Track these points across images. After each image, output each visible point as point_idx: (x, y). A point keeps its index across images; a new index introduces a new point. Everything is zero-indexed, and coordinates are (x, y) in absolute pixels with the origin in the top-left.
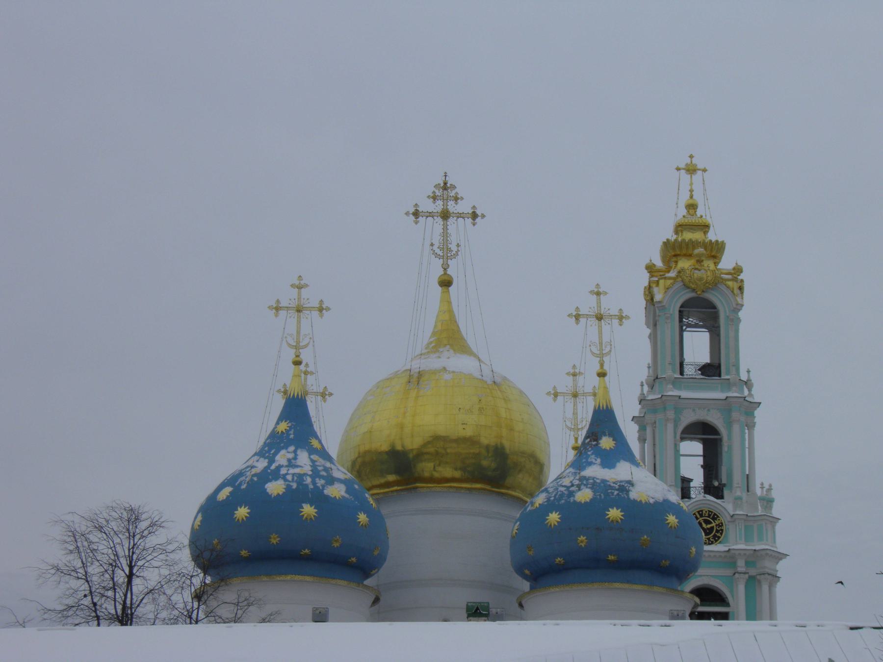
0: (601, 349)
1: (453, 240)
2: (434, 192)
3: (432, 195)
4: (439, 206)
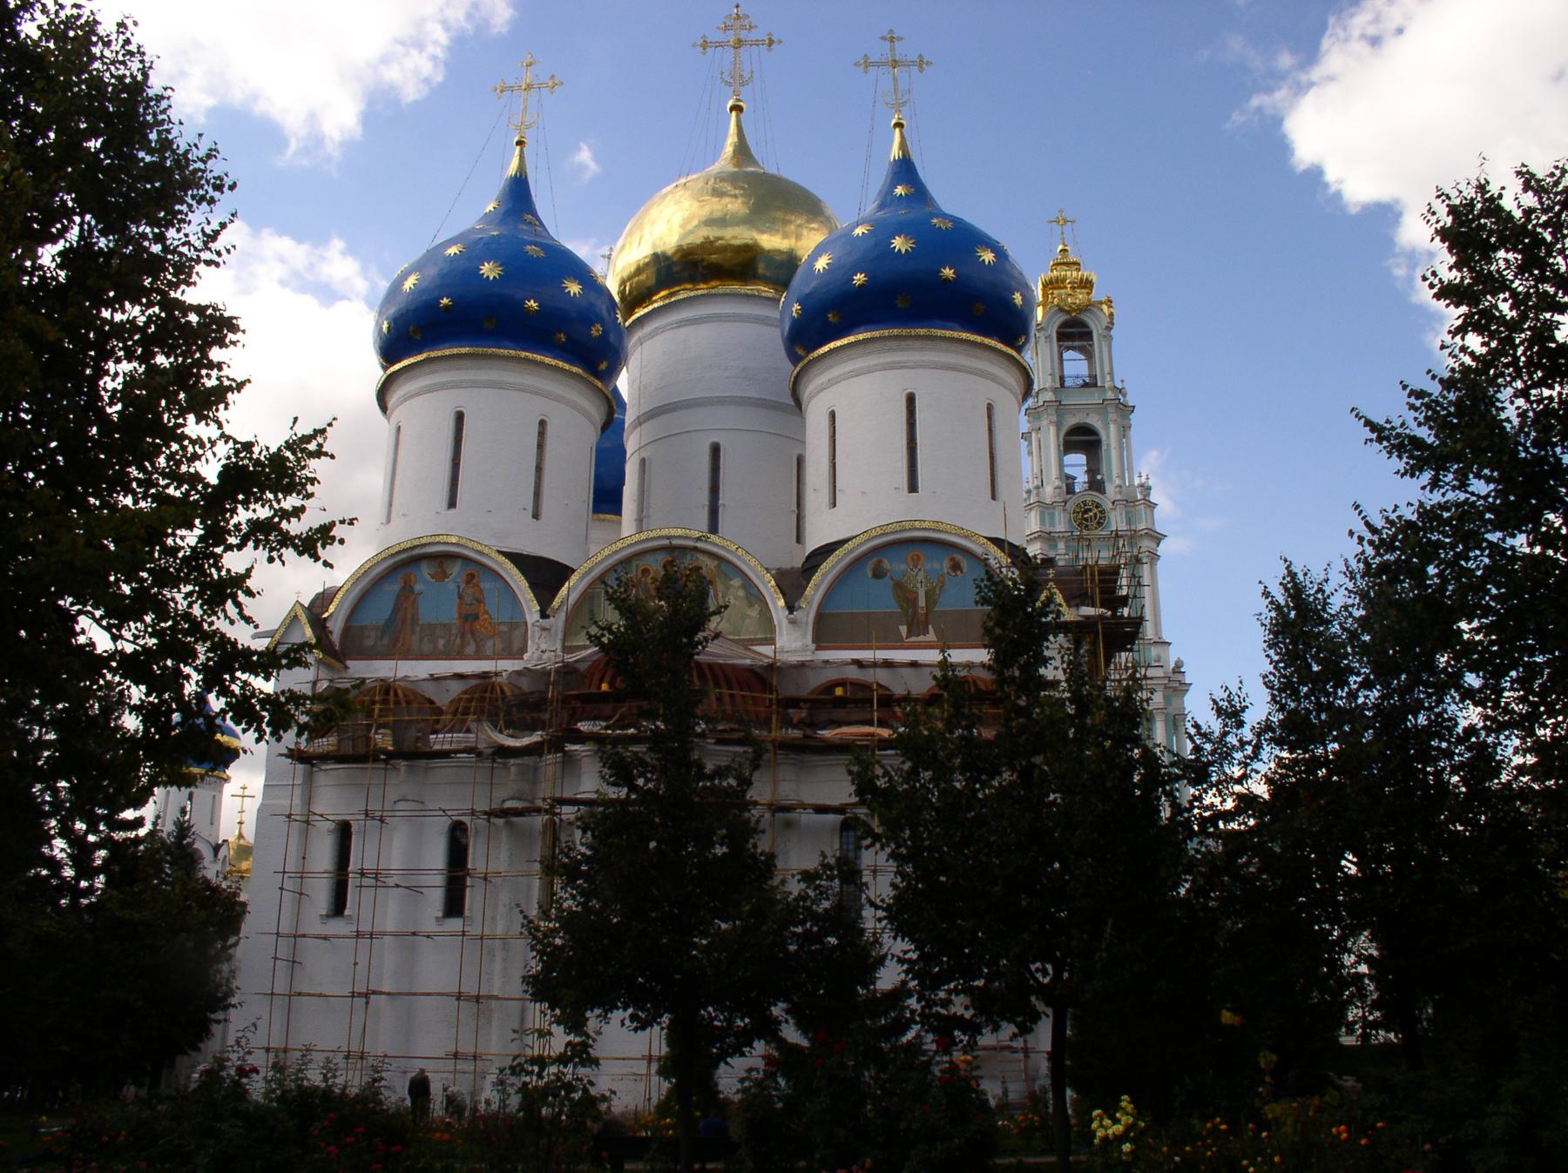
4: (731, 37)
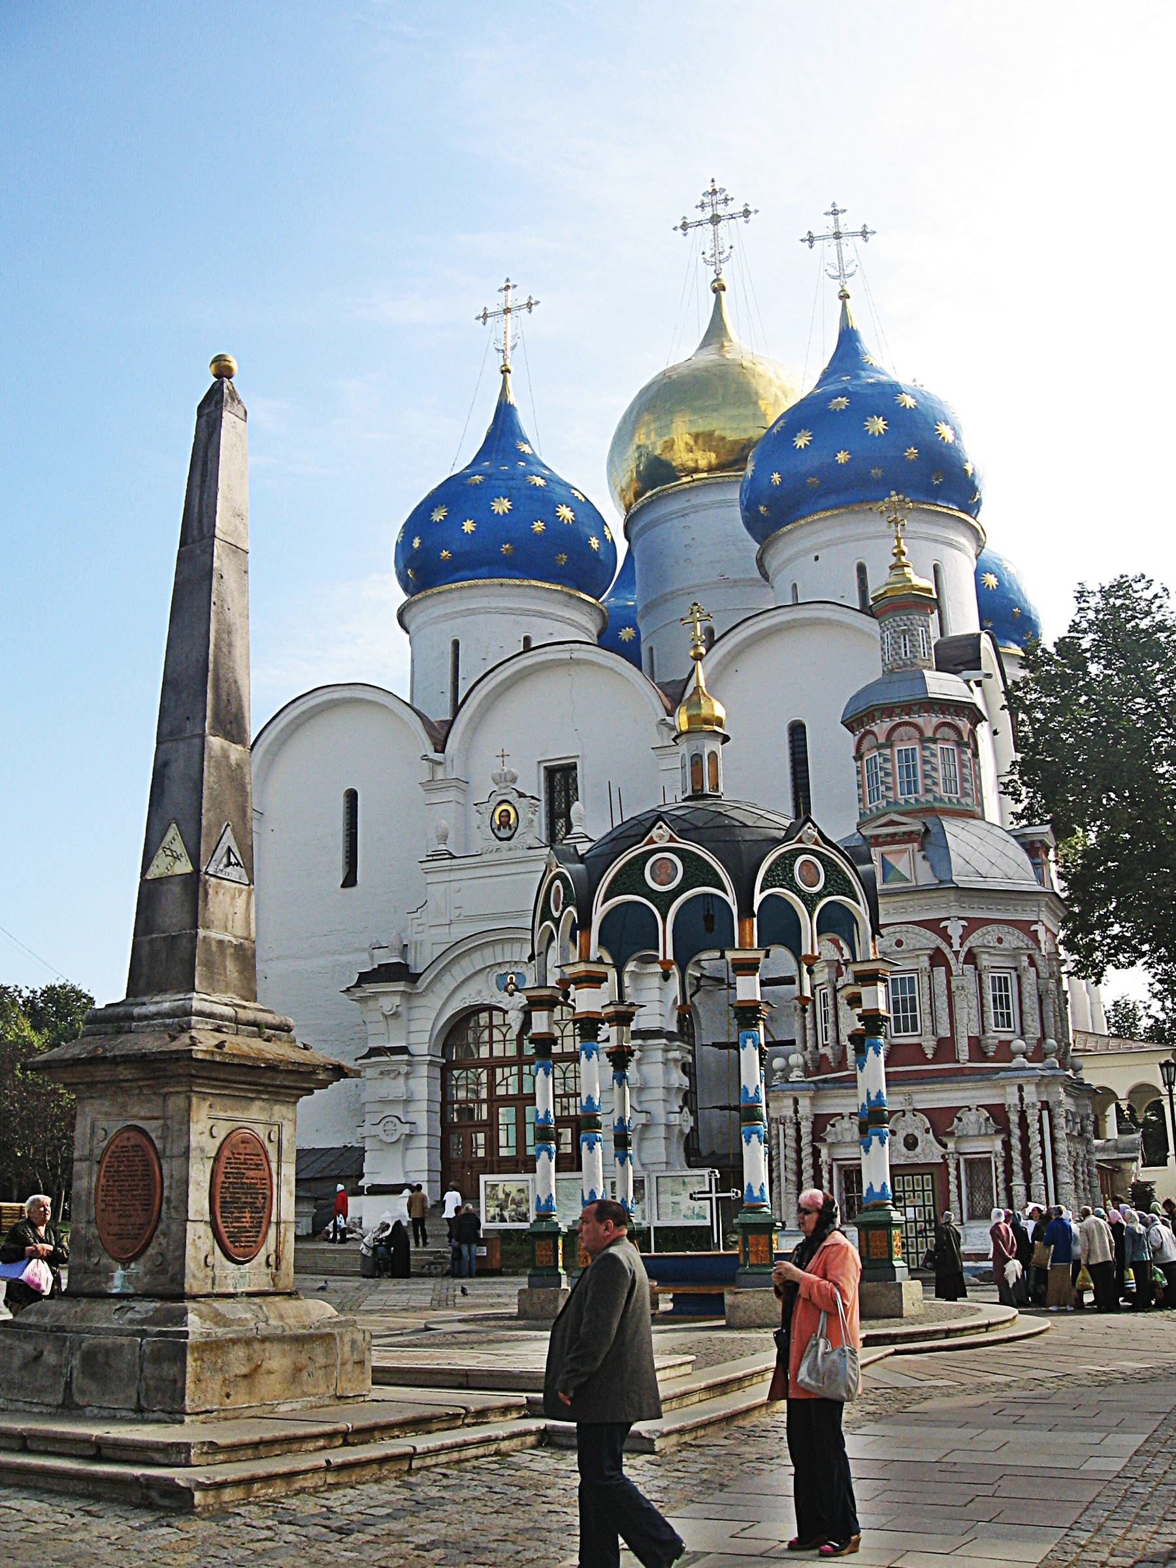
0: (841, 269)
1: (725, 244)
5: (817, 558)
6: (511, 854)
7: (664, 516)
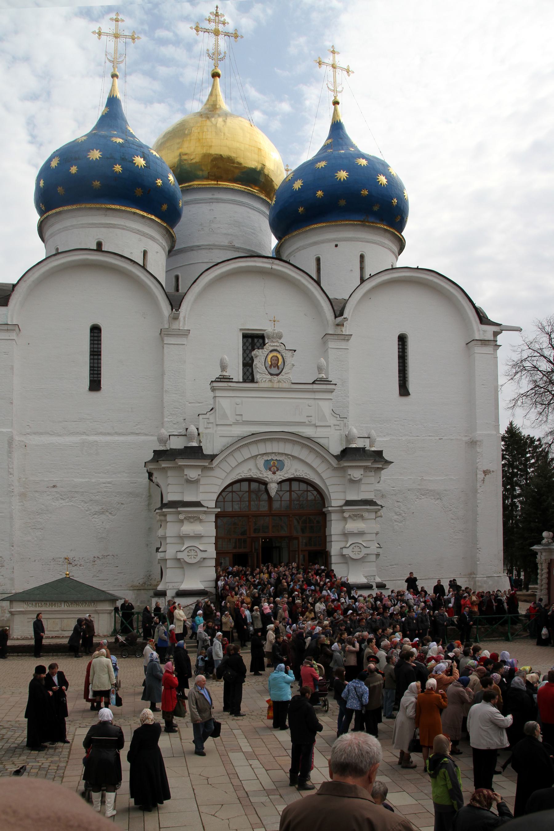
2: (209, 17)
3: (208, 18)
5: (336, 246)
6: (281, 385)
7: (196, 200)
